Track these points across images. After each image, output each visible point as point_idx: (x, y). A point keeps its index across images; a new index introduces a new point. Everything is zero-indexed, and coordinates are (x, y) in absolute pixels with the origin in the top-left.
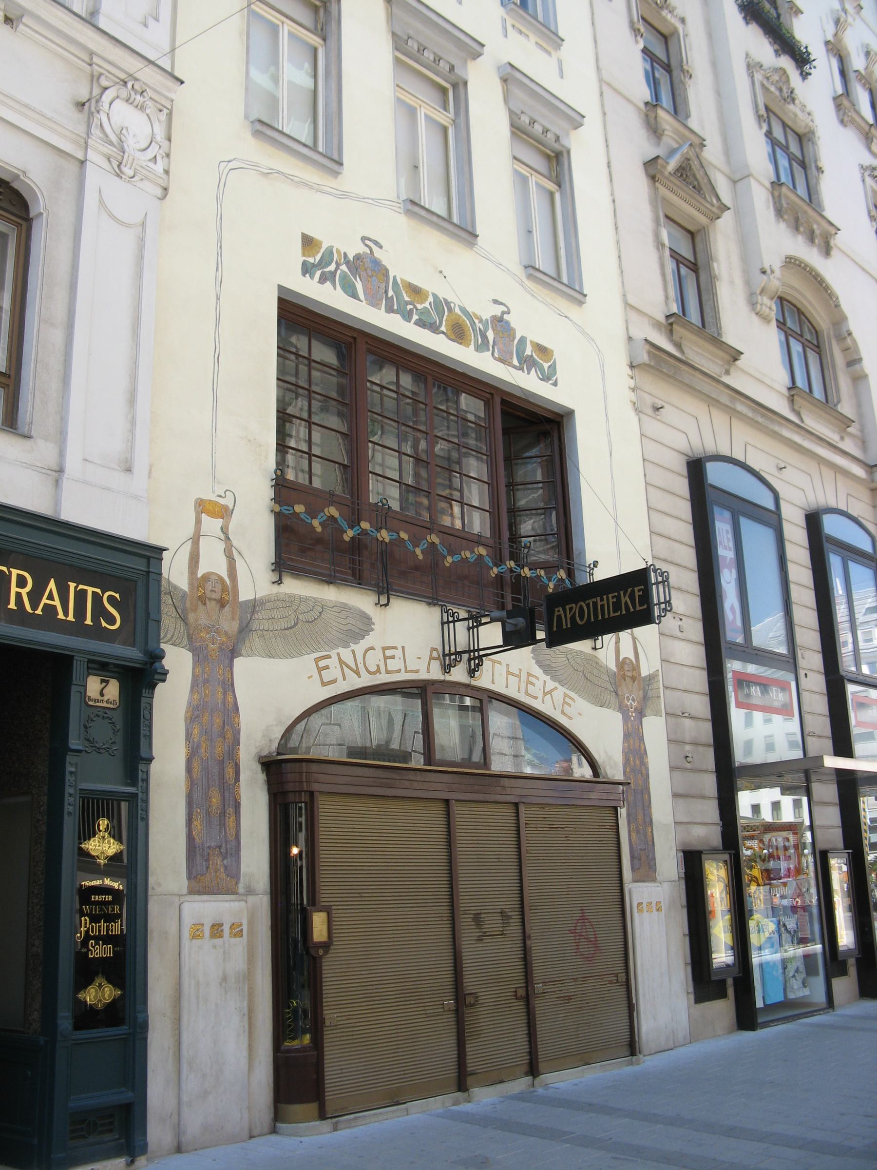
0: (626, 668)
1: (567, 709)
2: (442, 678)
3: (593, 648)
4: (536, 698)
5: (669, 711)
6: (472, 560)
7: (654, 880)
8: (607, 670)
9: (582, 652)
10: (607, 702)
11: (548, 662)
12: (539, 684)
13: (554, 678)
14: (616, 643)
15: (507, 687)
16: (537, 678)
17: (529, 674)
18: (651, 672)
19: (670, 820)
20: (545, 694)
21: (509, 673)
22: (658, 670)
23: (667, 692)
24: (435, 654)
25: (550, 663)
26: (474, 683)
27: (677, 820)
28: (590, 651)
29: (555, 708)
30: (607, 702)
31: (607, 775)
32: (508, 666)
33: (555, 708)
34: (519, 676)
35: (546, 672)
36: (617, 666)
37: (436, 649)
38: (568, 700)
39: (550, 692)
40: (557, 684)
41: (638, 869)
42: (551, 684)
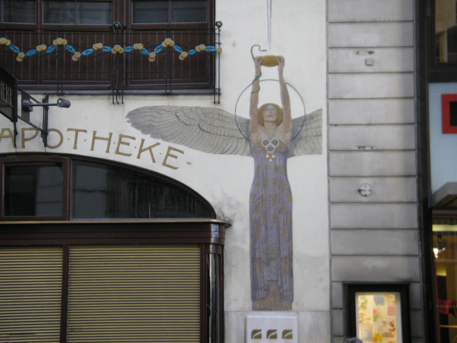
0: (267, 113)
1: (170, 161)
2: (13, 150)
3: (215, 102)
4: (129, 155)
5: (334, 146)
6: (49, 52)
7: (288, 308)
8: (236, 120)
9: (197, 108)
10: (232, 149)
11: (148, 123)
12: (138, 143)
13: (155, 136)
14: (253, 93)
15: (92, 149)
16: (134, 139)
17: (121, 136)
18: (308, 112)
19: (325, 251)
20: (141, 151)
21: (94, 138)
22: (320, 110)
23: (334, 129)
24: (6, 133)
25: (151, 122)
26: (49, 150)
27: (334, 252)
28: (214, 106)
29: (154, 161)
30: (232, 149)
31: (223, 214)
32: (95, 133)
33: (154, 161)
34: (109, 140)
35: (145, 131)
36: (251, 113)
37: (9, 130)
38: (172, 152)
39: (150, 148)
40: (160, 141)
41: (264, 299)
42: (149, 141)
